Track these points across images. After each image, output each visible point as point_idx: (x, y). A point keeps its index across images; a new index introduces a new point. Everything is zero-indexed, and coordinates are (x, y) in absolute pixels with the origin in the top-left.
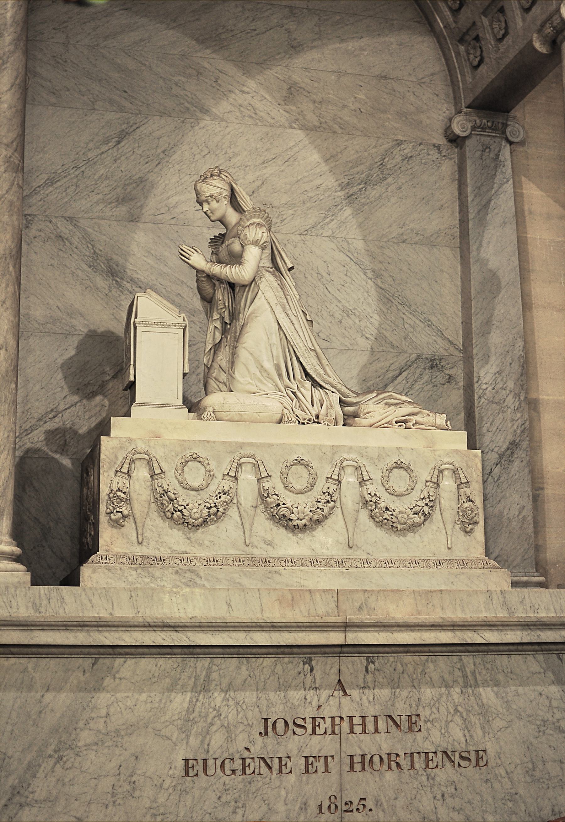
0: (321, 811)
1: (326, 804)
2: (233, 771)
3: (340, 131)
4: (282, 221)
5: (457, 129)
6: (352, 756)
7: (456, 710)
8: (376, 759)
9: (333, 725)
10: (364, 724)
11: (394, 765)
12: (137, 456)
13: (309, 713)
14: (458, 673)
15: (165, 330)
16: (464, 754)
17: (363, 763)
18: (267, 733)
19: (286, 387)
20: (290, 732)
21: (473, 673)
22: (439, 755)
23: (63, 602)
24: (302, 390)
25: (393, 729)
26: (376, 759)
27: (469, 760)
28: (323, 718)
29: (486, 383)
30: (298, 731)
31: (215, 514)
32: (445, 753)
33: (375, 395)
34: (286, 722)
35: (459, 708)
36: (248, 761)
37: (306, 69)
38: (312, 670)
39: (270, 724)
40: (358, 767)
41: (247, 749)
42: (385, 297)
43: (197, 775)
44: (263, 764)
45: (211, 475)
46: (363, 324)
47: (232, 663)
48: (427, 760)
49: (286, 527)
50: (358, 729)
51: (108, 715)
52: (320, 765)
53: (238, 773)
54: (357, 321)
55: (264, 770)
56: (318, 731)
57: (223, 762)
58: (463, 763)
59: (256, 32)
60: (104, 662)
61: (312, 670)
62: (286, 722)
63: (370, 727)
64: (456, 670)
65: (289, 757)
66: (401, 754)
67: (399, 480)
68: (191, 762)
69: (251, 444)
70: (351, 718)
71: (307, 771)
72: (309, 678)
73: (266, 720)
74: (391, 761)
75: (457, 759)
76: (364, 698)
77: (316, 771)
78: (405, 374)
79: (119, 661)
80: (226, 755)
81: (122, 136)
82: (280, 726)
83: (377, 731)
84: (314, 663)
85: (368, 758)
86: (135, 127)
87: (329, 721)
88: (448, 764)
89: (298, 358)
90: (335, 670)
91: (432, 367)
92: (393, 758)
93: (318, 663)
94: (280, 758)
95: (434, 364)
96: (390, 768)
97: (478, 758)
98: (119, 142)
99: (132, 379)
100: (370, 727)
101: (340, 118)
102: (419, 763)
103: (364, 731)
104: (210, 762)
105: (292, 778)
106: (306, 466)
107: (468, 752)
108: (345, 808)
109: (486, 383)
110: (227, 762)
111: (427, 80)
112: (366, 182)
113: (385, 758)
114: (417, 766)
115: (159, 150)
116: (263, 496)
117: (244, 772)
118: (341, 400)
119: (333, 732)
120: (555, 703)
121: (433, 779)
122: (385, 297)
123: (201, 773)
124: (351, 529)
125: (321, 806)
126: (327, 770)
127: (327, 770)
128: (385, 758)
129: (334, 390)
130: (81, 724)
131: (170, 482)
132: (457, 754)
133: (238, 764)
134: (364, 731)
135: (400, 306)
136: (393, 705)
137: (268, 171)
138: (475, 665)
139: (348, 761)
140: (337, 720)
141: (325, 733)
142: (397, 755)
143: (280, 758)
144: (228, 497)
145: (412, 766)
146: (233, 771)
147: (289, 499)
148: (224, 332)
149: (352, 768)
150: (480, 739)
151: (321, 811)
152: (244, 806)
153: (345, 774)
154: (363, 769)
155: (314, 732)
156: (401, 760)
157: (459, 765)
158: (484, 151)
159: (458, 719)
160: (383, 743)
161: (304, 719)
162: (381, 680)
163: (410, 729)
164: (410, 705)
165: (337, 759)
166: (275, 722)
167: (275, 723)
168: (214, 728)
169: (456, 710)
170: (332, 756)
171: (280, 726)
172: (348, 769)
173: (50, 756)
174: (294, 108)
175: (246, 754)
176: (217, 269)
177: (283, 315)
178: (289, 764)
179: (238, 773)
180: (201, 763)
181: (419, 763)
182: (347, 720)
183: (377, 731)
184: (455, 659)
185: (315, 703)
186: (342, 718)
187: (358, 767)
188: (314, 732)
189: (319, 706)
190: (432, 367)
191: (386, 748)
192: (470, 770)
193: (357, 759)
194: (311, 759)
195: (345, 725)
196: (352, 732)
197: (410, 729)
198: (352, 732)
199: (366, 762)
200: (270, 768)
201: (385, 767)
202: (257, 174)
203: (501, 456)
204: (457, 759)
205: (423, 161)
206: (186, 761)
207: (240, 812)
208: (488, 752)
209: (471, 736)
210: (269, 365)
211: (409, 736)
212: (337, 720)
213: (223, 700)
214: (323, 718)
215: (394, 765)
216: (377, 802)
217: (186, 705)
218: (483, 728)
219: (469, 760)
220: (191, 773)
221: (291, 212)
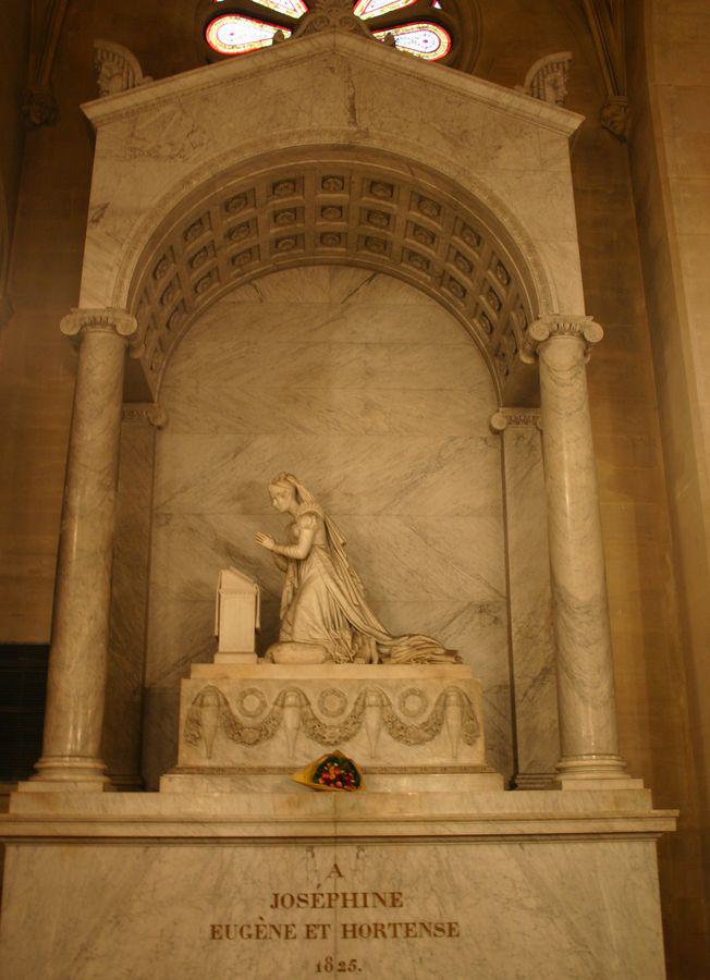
0: (319, 971)
1: (323, 963)
2: (250, 936)
3: (405, 434)
5: (497, 426)
6: (345, 926)
7: (432, 890)
8: (365, 929)
10: (355, 900)
11: (379, 933)
13: (310, 890)
14: (433, 859)
16: (439, 926)
17: (354, 931)
20: (295, 905)
22: (418, 926)
23: (133, 804)
25: (379, 904)
26: (365, 929)
28: (322, 895)
30: (302, 904)
35: (435, 888)
36: (261, 928)
37: (379, 389)
38: (313, 856)
39: (279, 898)
40: (350, 934)
41: (261, 918)
44: (273, 931)
45: (264, 704)
47: (249, 852)
48: (408, 930)
49: (321, 743)
50: (350, 904)
51: (155, 890)
52: (319, 932)
54: (420, 579)
55: (274, 935)
56: (318, 905)
57: (241, 930)
58: (438, 933)
60: (153, 850)
61: (313, 856)
62: (292, 897)
63: (360, 902)
66: (386, 924)
68: (217, 928)
69: (295, 681)
70: (344, 895)
72: (311, 863)
74: (377, 930)
75: (433, 930)
78: (458, 618)
79: (164, 849)
81: (238, 451)
82: (287, 901)
83: (365, 906)
84: (315, 850)
85: (357, 927)
87: (326, 896)
88: (425, 934)
90: (332, 856)
91: (481, 612)
92: (379, 927)
94: (287, 927)
96: (376, 936)
97: (451, 929)
98: (235, 456)
99: (216, 634)
100: (360, 902)
102: (401, 932)
103: (355, 906)
104: (232, 929)
107: (442, 924)
108: (339, 967)
110: (244, 929)
112: (426, 471)
113: (373, 928)
114: (399, 934)
116: (303, 719)
117: (258, 937)
119: (330, 906)
120: (518, 885)
121: (413, 945)
123: (224, 937)
124: (373, 744)
125: (319, 966)
126: (324, 937)
127: (324, 937)
128: (373, 928)
130: (134, 897)
133: (253, 931)
134: (355, 906)
136: (379, 885)
138: (448, 852)
139: (342, 929)
140: (333, 897)
143: (287, 927)
144: (276, 720)
145: (395, 936)
146: (250, 936)
147: (325, 720)
148: (294, 594)
149: (345, 936)
150: (452, 914)
151: (319, 971)
152: (257, 964)
154: (354, 936)
155: (314, 906)
156: (386, 930)
157: (435, 935)
158: (519, 438)
159: (433, 897)
162: (369, 864)
163: (394, 905)
164: (394, 885)
165: (332, 927)
167: (283, 900)
168: (235, 901)
171: (287, 901)
172: (342, 935)
173: (111, 921)
174: (369, 420)
175: (260, 922)
176: (280, 549)
177: (329, 580)
178: (294, 931)
179: (254, 937)
180: (224, 928)
181: (401, 932)
182: (341, 896)
183: (365, 906)
184: (431, 848)
185: (316, 882)
186: (337, 895)
187: (350, 934)
188: (314, 906)
189: (319, 886)
190: (481, 612)
191: (373, 919)
192: (444, 940)
193: (349, 928)
196: (345, 906)
199: (355, 931)
200: (279, 934)
201: (372, 935)
203: (535, 680)
204: (433, 930)
206: (213, 927)
207: (254, 968)
210: (319, 618)
211: (393, 910)
212: (333, 897)
214: (322, 895)
215: (379, 934)
216: (365, 963)
218: (455, 904)
220: (217, 936)
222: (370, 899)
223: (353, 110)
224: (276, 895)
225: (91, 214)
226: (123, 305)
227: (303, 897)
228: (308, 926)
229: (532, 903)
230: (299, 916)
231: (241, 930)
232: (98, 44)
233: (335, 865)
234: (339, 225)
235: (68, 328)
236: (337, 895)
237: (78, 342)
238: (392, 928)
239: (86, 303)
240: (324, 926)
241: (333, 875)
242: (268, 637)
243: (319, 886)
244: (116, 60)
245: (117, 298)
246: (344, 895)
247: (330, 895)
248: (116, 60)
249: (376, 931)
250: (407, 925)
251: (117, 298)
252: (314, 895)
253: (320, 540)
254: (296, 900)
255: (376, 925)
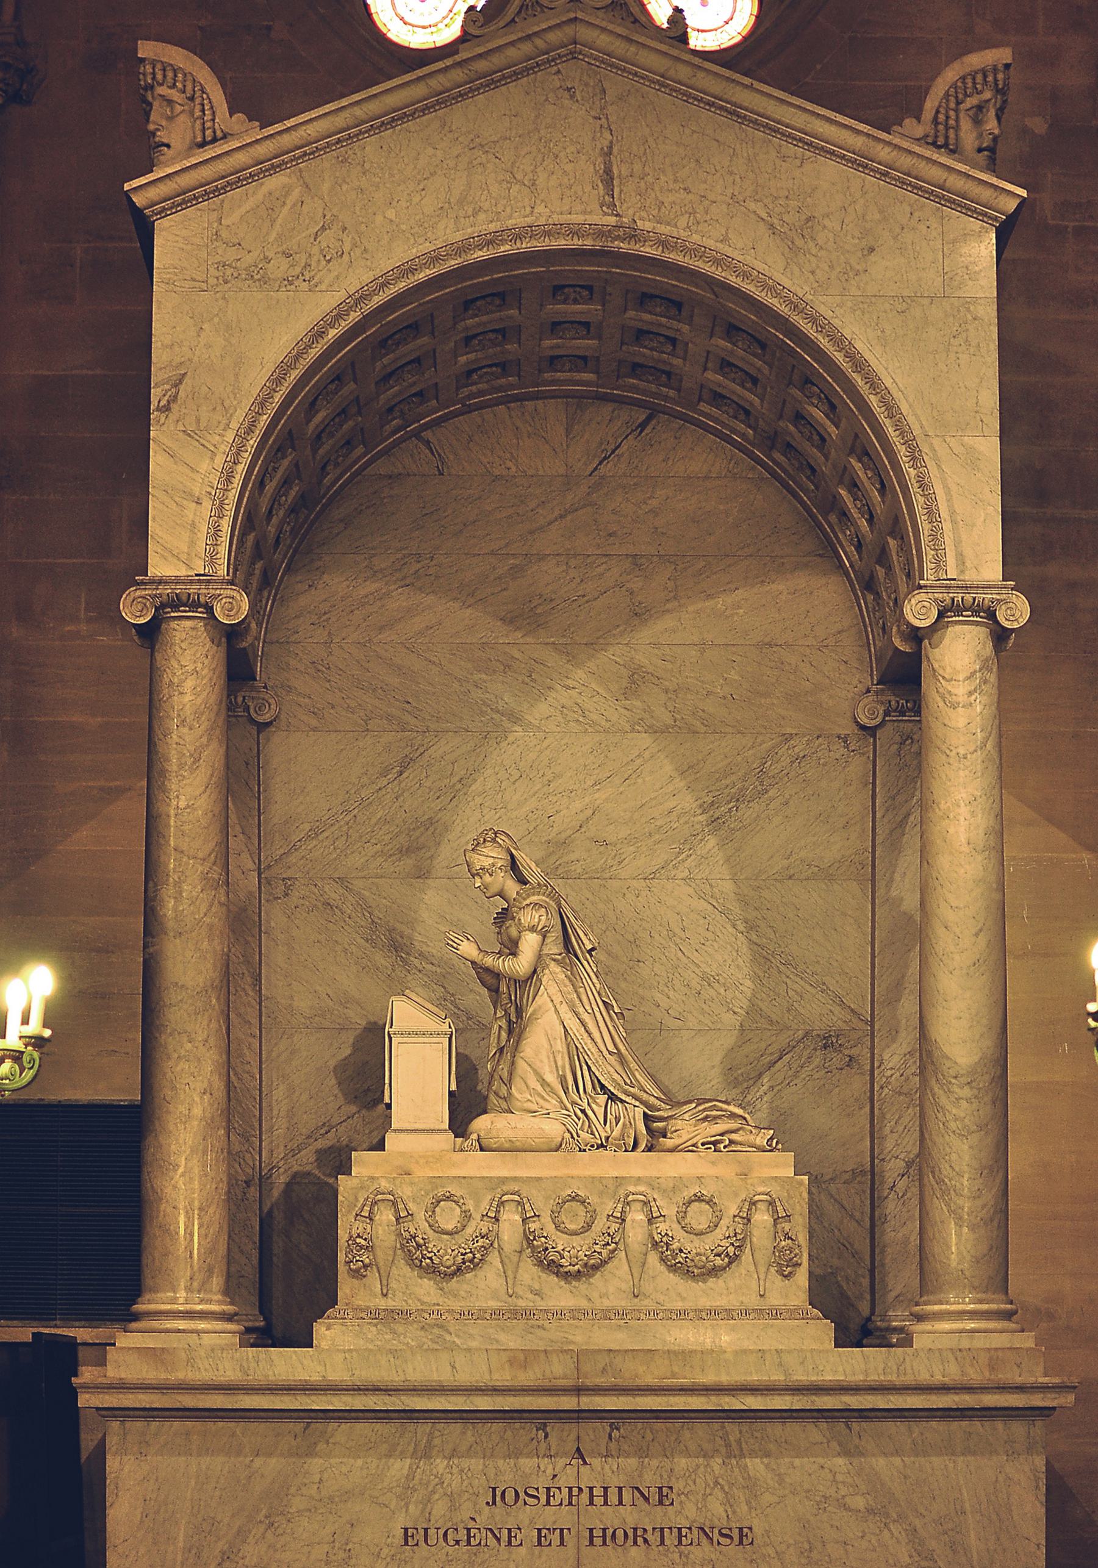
3: (703, 729)
4: (620, 863)
6: (591, 1530)
7: (716, 1483)
8: (620, 1534)
9: (570, 1496)
10: (605, 1496)
11: (640, 1540)
12: (380, 1197)
13: (542, 1482)
15: (421, 1040)
16: (724, 1531)
17: (604, 1536)
18: (494, 1503)
19: (574, 1103)
20: (521, 1502)
21: (739, 1442)
22: (695, 1531)
23: (283, 1363)
24: (593, 1106)
25: (640, 1501)
26: (620, 1534)
27: (731, 1538)
28: (559, 1488)
29: (892, 1069)
31: (471, 1261)
32: (702, 1529)
33: (694, 1105)
34: (516, 1492)
35: (720, 1480)
36: (473, 1532)
37: (656, 645)
38: (546, 1436)
39: (498, 1493)
40: (598, 1541)
42: (761, 955)
43: (417, 1545)
45: (467, 1216)
46: (729, 995)
47: (456, 1428)
49: (557, 1274)
51: (321, 1481)
52: (555, 1538)
53: (463, 1543)
54: (722, 991)
55: (492, 1541)
57: (446, 1532)
58: (722, 1540)
59: (586, 598)
60: (318, 1426)
61: (546, 1436)
62: (516, 1492)
63: (613, 1498)
64: (717, 1439)
65: (519, 1529)
66: (649, 1528)
67: (699, 1217)
69: (515, 1179)
70: (591, 1489)
71: (540, 1544)
72: (543, 1445)
73: (494, 1489)
75: (716, 1537)
76: (607, 1467)
77: (550, 1544)
78: (786, 1058)
79: (333, 1425)
80: (449, 1525)
81: (405, 764)
82: (510, 1496)
83: (620, 1503)
84: (548, 1429)
86: (421, 750)
87: (565, 1491)
89: (589, 1068)
90: (573, 1436)
91: (825, 1047)
92: (640, 1532)
93: (554, 1429)
95: (828, 1042)
96: (635, 1543)
100: (613, 1498)
101: (703, 711)
102: (670, 1539)
103: (606, 1503)
105: (523, 1550)
106: (583, 1202)
107: (730, 1529)
109: (892, 1069)
111: (831, 641)
112: (738, 799)
113: (630, 1533)
114: (667, 1542)
115: (456, 779)
116: (529, 1239)
117: (469, 1543)
118: (644, 1113)
119: (570, 1504)
120: (839, 1478)
121: (687, 1557)
122: (761, 955)
123: (422, 1543)
124: (636, 1275)
128: (630, 1533)
129: (637, 1103)
130: (293, 1490)
131: (420, 1225)
132: (716, 1531)
133: (462, 1535)
134: (606, 1503)
135: (782, 968)
136: (640, 1476)
137: (600, 796)
138: (740, 1432)
140: (575, 1491)
141: (561, 1504)
142: (645, 1530)
143: (509, 1530)
144: (490, 1241)
145: (662, 1542)
146: (457, 1542)
147: (561, 1242)
148: (510, 1032)
149: (591, 1543)
150: (744, 1515)
153: (583, 1548)
154: (604, 1543)
155: (548, 1503)
156: (649, 1536)
157: (719, 1543)
158: (902, 743)
159: (717, 1492)
160: (629, 1516)
161: (537, 1489)
162: (626, 1448)
163: (661, 1503)
164: (661, 1476)
166: (504, 1491)
167: (503, 1493)
168: (436, 1496)
169: (716, 1483)
170: (569, 1529)
171: (510, 1496)
173: (261, 1522)
174: (638, 704)
175: (471, 1524)
176: (489, 961)
177: (570, 1015)
180: (422, 1532)
181: (670, 1539)
182: (586, 1491)
183: (620, 1503)
184: (716, 1426)
185: (550, 1472)
186: (580, 1490)
187: (598, 1541)
188: (548, 1503)
189: (555, 1476)
190: (825, 1047)
191: (631, 1522)
192: (732, 1550)
194: (544, 1532)
195: (585, 1497)
196: (591, 1503)
197: (661, 1503)
198: (591, 1503)
200: (498, 1540)
201: (630, 1541)
202: (587, 800)
204: (716, 1537)
205: (822, 761)
206: (406, 1530)
208: (755, 1529)
209: (734, 1512)
210: (551, 1078)
212: (575, 1491)
213: (447, 1467)
215: (640, 1540)
217: (405, 1472)
218: (748, 1503)
219: (731, 1538)
221: (632, 849)
222: (626, 1496)
223: (608, 178)
224: (494, 1489)
225: (156, 394)
226: (222, 571)
227: (531, 1492)
228: (539, 1530)
229: (859, 1502)
230: (526, 1516)
231: (445, 1534)
232: (146, 49)
233: (578, 1449)
234: (586, 345)
235: (134, 610)
236: (580, 1490)
237: (150, 633)
238: (658, 1534)
239: (159, 566)
240: (562, 1530)
241: (574, 1462)
242: (466, 1106)
243: (555, 1476)
244: (182, 79)
245: (212, 560)
246: (591, 1489)
247: (570, 1489)
248: (182, 79)
249: (635, 1536)
250: (680, 1529)
251: (212, 560)
252: (548, 1489)
253: (554, 947)
254: (522, 1494)
255: (635, 1529)
